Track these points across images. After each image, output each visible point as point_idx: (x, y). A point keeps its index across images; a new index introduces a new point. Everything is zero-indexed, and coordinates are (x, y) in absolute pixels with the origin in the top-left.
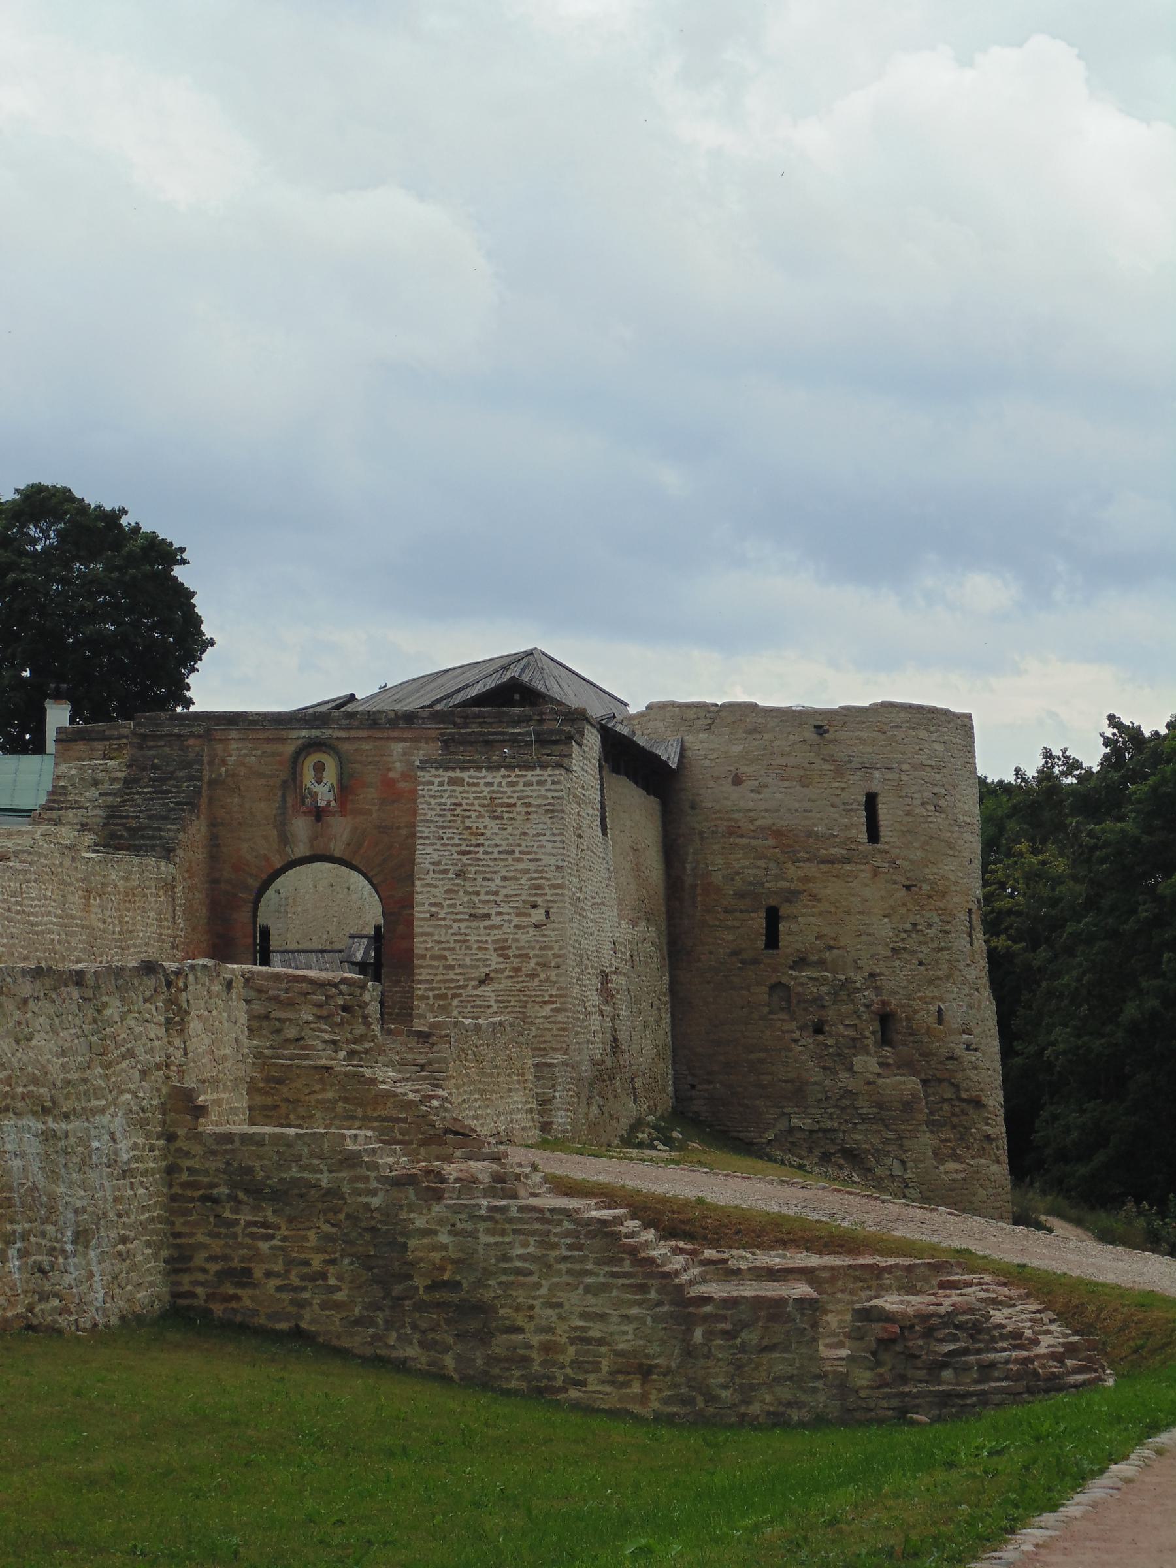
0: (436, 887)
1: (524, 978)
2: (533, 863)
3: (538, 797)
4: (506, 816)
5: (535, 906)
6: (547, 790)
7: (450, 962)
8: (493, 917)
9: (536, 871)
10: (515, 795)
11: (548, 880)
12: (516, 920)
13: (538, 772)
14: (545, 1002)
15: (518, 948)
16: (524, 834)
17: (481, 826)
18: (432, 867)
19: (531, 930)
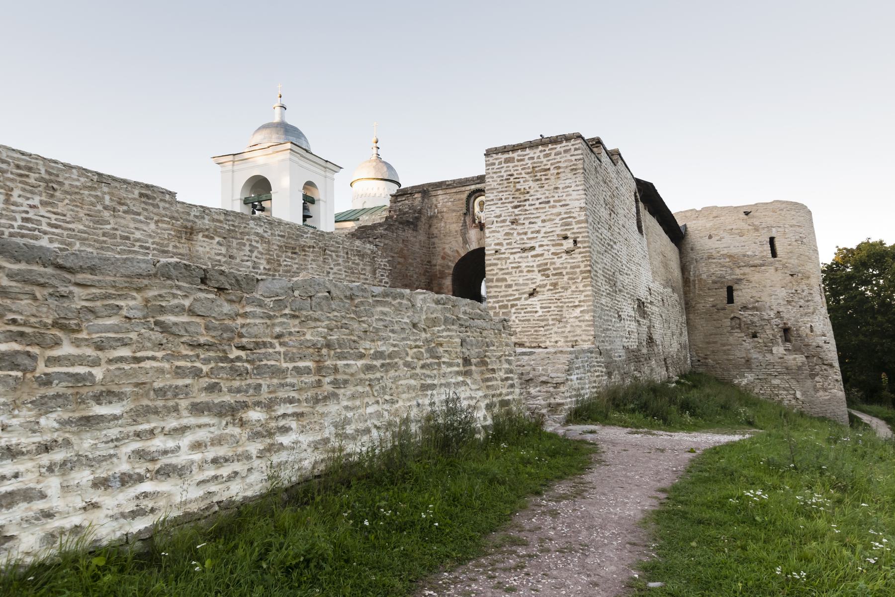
0: (498, 232)
1: (560, 290)
3: (565, 161)
4: (543, 178)
5: (566, 238)
7: (509, 282)
8: (537, 249)
9: (566, 213)
10: (549, 163)
11: (574, 218)
12: (553, 250)
13: (564, 144)
14: (576, 306)
15: (554, 269)
16: (556, 188)
17: (527, 187)
18: (495, 219)
19: (564, 256)
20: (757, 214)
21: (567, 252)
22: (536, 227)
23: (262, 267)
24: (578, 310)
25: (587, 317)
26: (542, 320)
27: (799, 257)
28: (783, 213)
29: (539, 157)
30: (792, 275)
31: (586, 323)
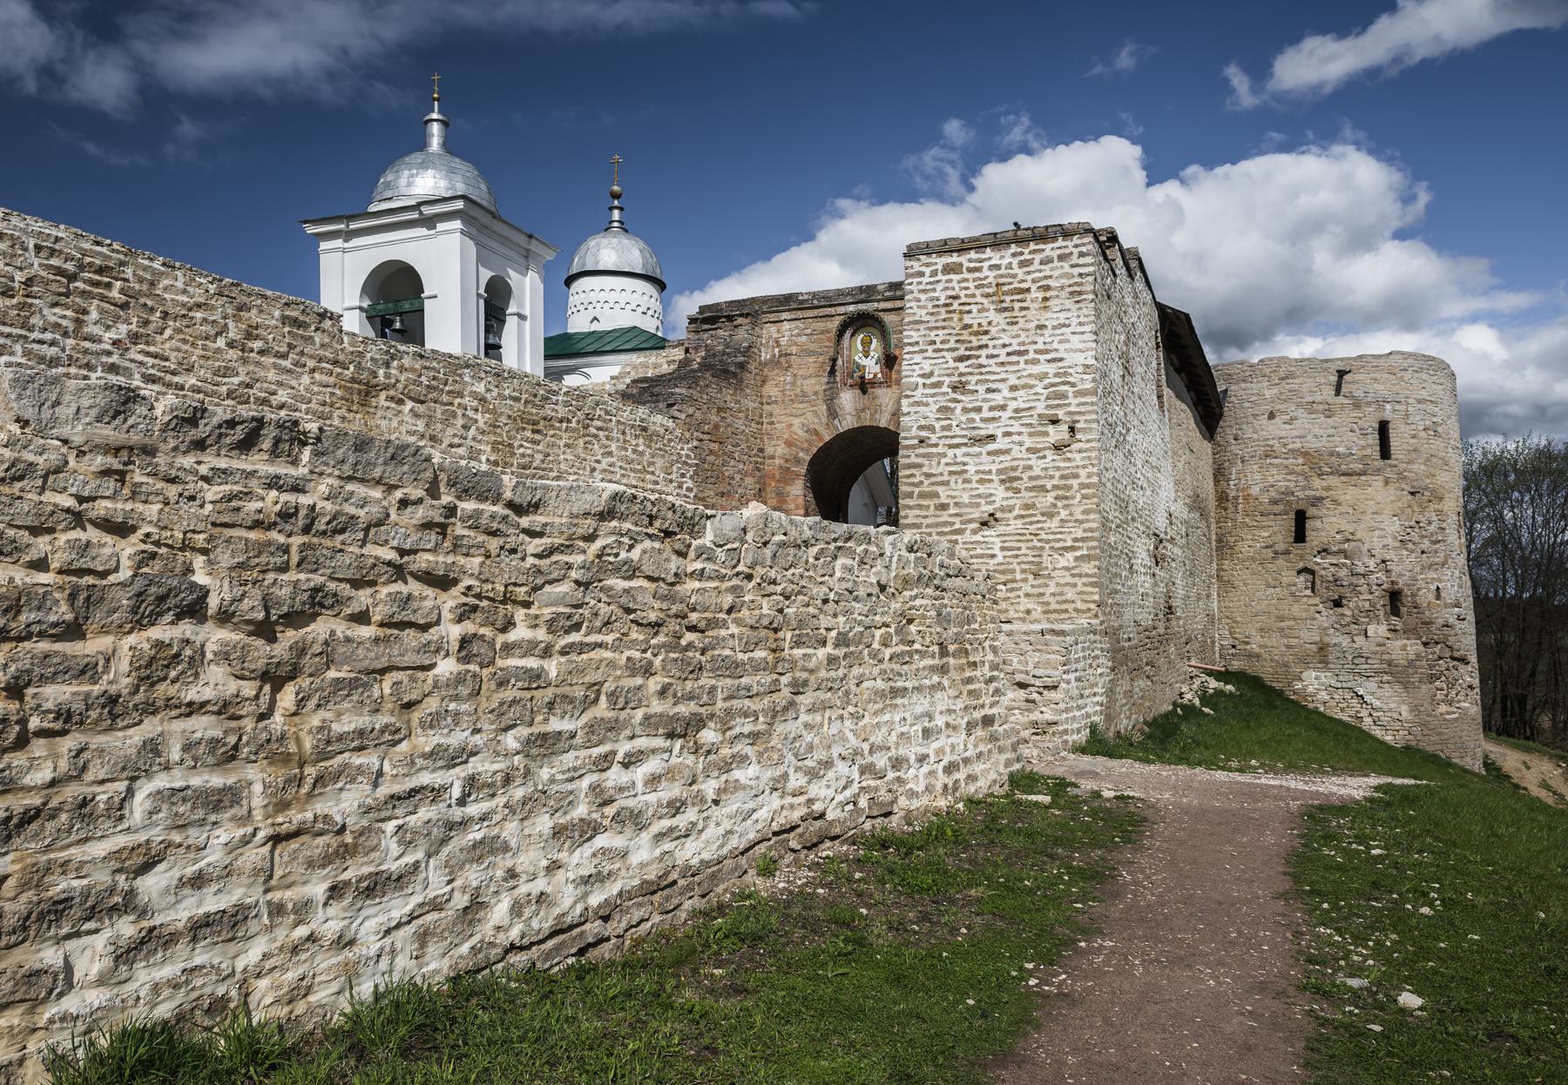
0: (927, 405)
1: (1039, 518)
2: (1054, 365)
3: (1061, 276)
4: (1017, 305)
5: (1055, 422)
6: (1072, 266)
7: (944, 500)
8: (999, 439)
9: (1057, 375)
10: (1029, 278)
11: (1073, 385)
13: (1060, 243)
14: (1067, 549)
15: (1031, 478)
16: (1041, 327)
17: (985, 323)
18: (921, 381)
19: (1050, 455)
20: (1357, 377)
21: (1057, 448)
22: (998, 399)
23: (483, 458)
24: (1070, 556)
25: (1089, 568)
26: (1003, 572)
27: (1427, 460)
28: (1407, 376)
29: (1009, 266)
30: (1412, 494)
31: (1085, 580)
